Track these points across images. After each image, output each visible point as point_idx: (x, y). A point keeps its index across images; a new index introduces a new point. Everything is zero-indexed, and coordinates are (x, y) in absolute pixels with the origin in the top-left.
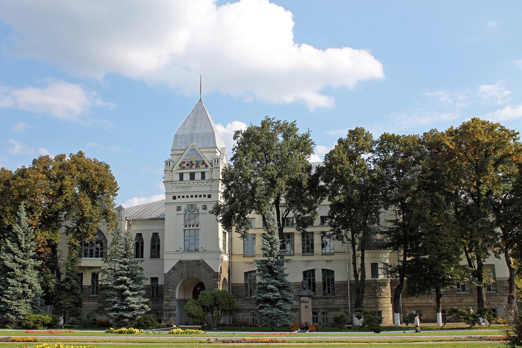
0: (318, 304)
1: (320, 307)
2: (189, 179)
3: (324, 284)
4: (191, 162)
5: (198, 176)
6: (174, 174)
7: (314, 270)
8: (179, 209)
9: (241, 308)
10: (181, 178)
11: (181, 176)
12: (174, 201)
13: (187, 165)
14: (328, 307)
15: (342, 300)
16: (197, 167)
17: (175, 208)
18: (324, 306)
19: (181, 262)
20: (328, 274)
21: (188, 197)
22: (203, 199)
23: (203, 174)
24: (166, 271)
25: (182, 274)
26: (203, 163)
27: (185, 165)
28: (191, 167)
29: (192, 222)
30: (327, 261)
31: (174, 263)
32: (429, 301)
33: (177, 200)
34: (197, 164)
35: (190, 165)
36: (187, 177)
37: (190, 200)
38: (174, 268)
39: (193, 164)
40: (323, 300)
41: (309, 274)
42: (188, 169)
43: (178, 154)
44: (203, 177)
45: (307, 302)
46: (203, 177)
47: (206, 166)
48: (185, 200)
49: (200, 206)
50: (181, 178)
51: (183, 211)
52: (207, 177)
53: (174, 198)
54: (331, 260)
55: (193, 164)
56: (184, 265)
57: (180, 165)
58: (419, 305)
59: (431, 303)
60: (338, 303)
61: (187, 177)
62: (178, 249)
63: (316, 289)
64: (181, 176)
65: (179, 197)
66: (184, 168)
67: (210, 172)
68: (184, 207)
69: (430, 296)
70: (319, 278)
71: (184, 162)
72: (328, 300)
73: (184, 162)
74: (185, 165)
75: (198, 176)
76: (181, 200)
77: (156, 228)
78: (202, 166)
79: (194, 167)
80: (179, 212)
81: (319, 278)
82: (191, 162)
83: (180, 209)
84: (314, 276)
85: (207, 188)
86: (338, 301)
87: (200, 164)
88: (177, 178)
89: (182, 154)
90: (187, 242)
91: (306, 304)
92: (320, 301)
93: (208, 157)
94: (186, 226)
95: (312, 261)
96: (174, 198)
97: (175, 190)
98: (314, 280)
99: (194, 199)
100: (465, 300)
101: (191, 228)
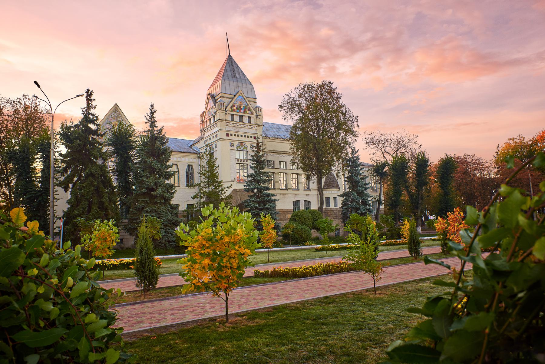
4: (240, 107)
5: (246, 120)
8: (232, 145)
10: (232, 119)
11: (232, 115)
12: (228, 138)
13: (237, 108)
16: (244, 112)
17: (228, 143)
21: (238, 136)
22: (250, 139)
23: (249, 118)
25: (236, 201)
26: (249, 110)
28: (240, 112)
30: (307, 195)
33: (230, 138)
34: (245, 109)
35: (239, 108)
36: (237, 119)
37: (240, 138)
39: (241, 109)
41: (296, 203)
43: (227, 98)
44: (249, 122)
46: (249, 122)
47: (252, 113)
48: (236, 138)
49: (248, 145)
51: (235, 148)
52: (252, 122)
55: (241, 109)
56: (238, 193)
57: (231, 108)
61: (237, 119)
64: (232, 115)
65: (231, 135)
66: (234, 111)
67: (255, 117)
68: (236, 144)
70: (302, 207)
71: (234, 106)
73: (234, 106)
74: (235, 108)
75: (246, 120)
76: (233, 138)
77: (175, 159)
78: (248, 112)
79: (242, 111)
80: (232, 148)
83: (233, 146)
85: (253, 131)
87: (247, 110)
88: (229, 118)
89: (232, 99)
93: (252, 105)
94: (238, 160)
96: (228, 135)
97: (228, 128)
99: (243, 139)
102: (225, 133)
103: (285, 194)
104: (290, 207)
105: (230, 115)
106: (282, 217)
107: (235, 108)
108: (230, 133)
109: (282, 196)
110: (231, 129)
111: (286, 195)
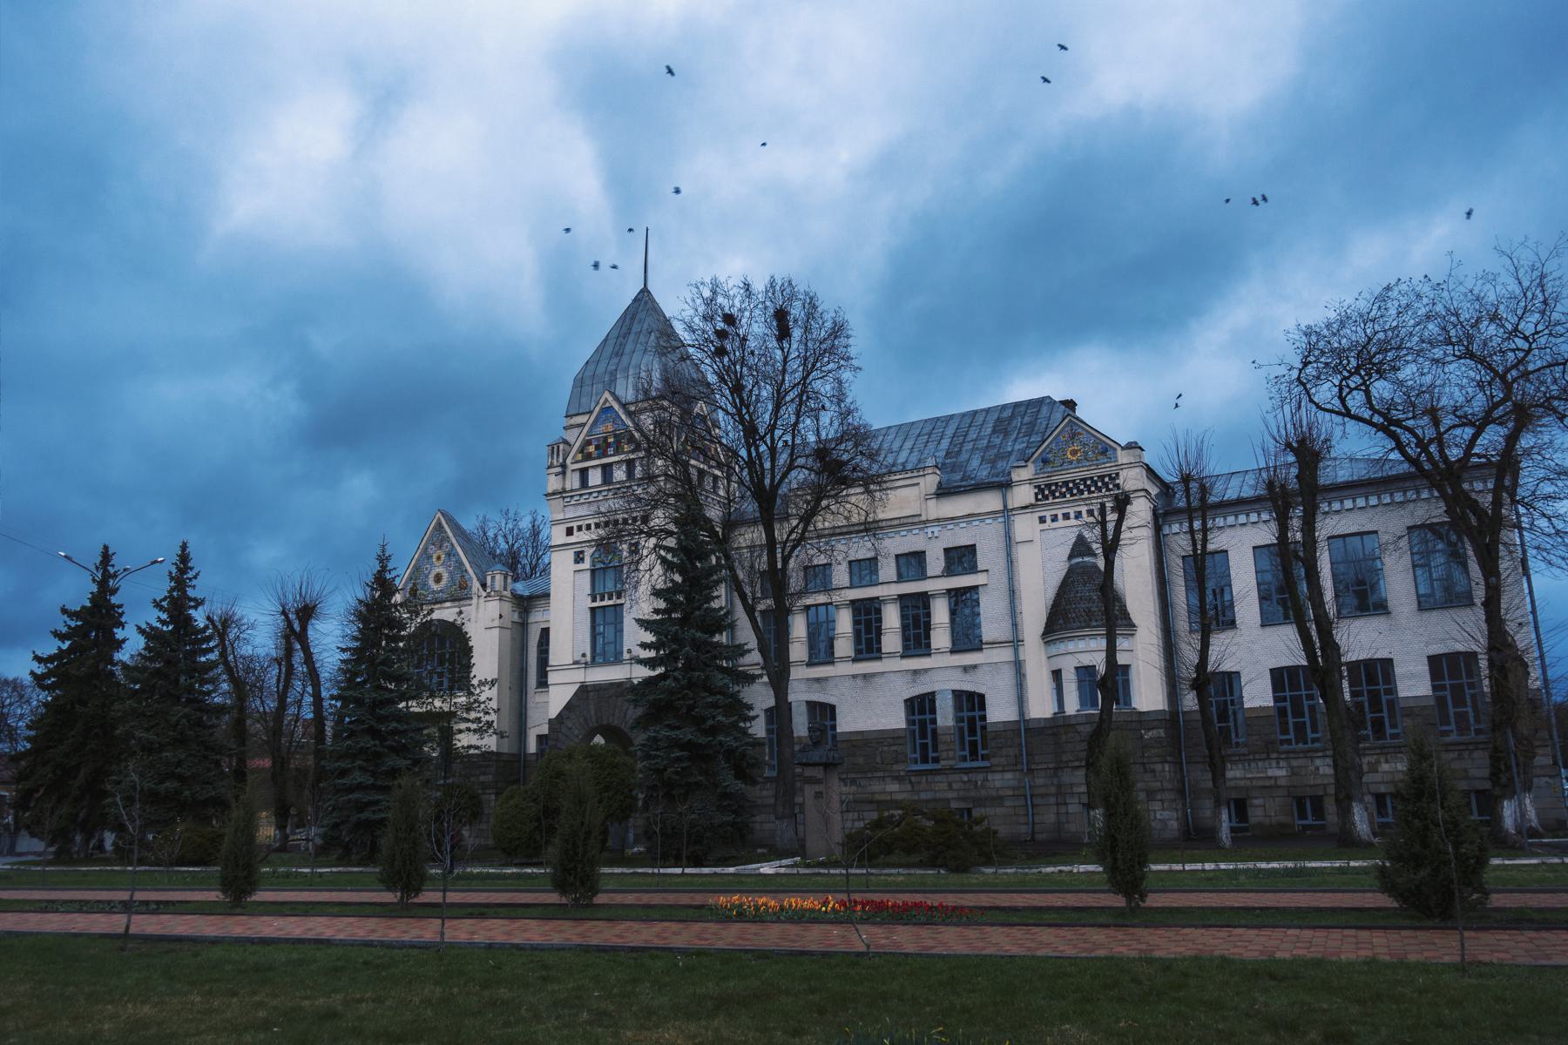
0: (944, 786)
1: (950, 795)
2: (599, 482)
3: (961, 730)
4: (606, 439)
6: (569, 473)
7: (933, 694)
8: (579, 558)
9: (759, 802)
10: (584, 482)
11: (584, 473)
13: (597, 448)
14: (973, 794)
15: (1009, 776)
18: (962, 794)
19: (584, 690)
20: (971, 702)
24: (553, 712)
27: (591, 449)
28: (605, 455)
29: (610, 586)
31: (570, 692)
32: (1270, 773)
33: (578, 537)
36: (595, 478)
38: (569, 707)
39: (609, 445)
40: (956, 777)
41: (921, 706)
42: (599, 458)
45: (819, 782)
50: (584, 482)
51: (587, 564)
53: (570, 532)
54: (975, 667)
55: (609, 445)
57: (581, 450)
58: (1242, 783)
59: (1276, 778)
60: (998, 784)
61: (595, 478)
62: (578, 657)
63: (941, 747)
65: (580, 528)
66: (588, 457)
68: (589, 552)
69: (1274, 755)
70: (945, 716)
71: (589, 443)
72: (973, 776)
78: (626, 448)
80: (581, 566)
81: (945, 716)
82: (606, 439)
83: (582, 560)
84: (933, 711)
86: (998, 776)
88: (573, 481)
90: (600, 640)
91: (818, 788)
92: (952, 777)
94: (594, 600)
95: (926, 670)
96: (570, 532)
97: (570, 513)
98: (934, 721)
100: (1385, 767)
101: (606, 602)
102: (562, 528)
103: (873, 675)
104: (896, 720)
105: (577, 475)
106: (861, 760)
107: (591, 449)
108: (575, 525)
109: (859, 682)
110: (583, 511)
111: (877, 680)
